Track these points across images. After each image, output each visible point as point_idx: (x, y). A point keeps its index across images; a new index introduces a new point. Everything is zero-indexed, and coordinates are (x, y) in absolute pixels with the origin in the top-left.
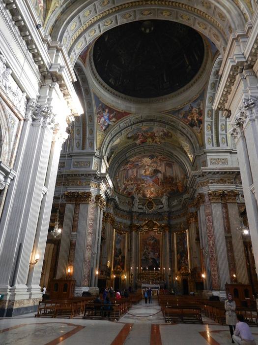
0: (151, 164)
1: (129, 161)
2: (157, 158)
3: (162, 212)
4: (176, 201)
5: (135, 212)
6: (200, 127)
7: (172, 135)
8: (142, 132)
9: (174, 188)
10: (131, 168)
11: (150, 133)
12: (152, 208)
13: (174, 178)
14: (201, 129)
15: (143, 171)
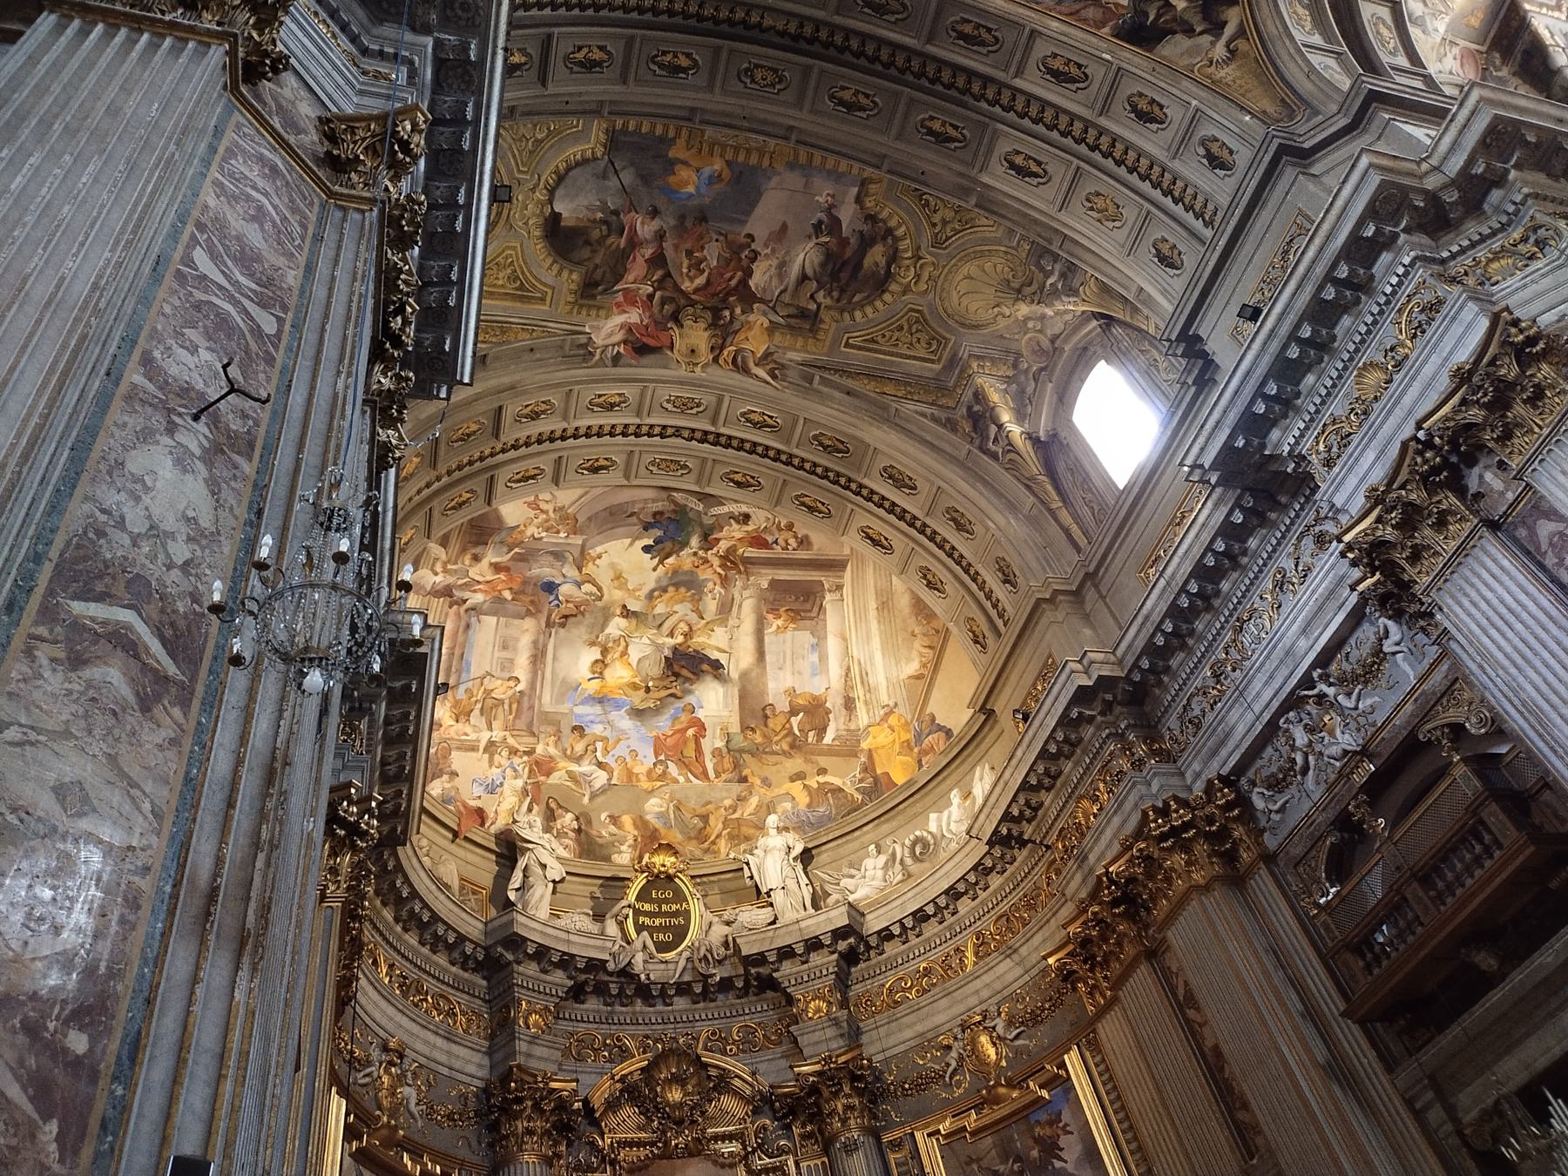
0: (650, 596)
1: (499, 519)
2: (708, 541)
3: (786, 953)
4: (874, 865)
5: (542, 953)
6: (1217, 28)
7: (893, 257)
8: (668, 221)
9: (837, 781)
10: (497, 606)
11: (712, 253)
12: (681, 933)
13: (834, 702)
14: (1241, 33)
15: (595, 654)
